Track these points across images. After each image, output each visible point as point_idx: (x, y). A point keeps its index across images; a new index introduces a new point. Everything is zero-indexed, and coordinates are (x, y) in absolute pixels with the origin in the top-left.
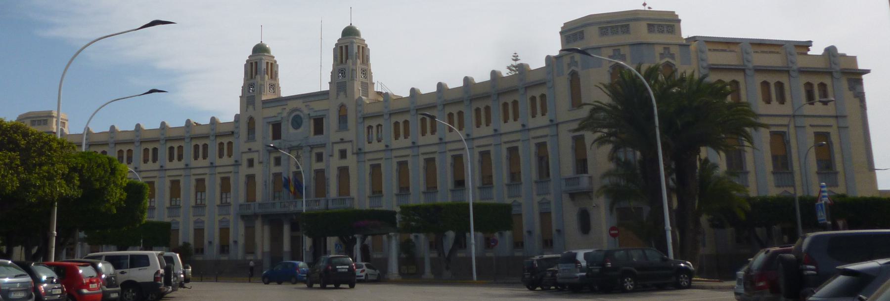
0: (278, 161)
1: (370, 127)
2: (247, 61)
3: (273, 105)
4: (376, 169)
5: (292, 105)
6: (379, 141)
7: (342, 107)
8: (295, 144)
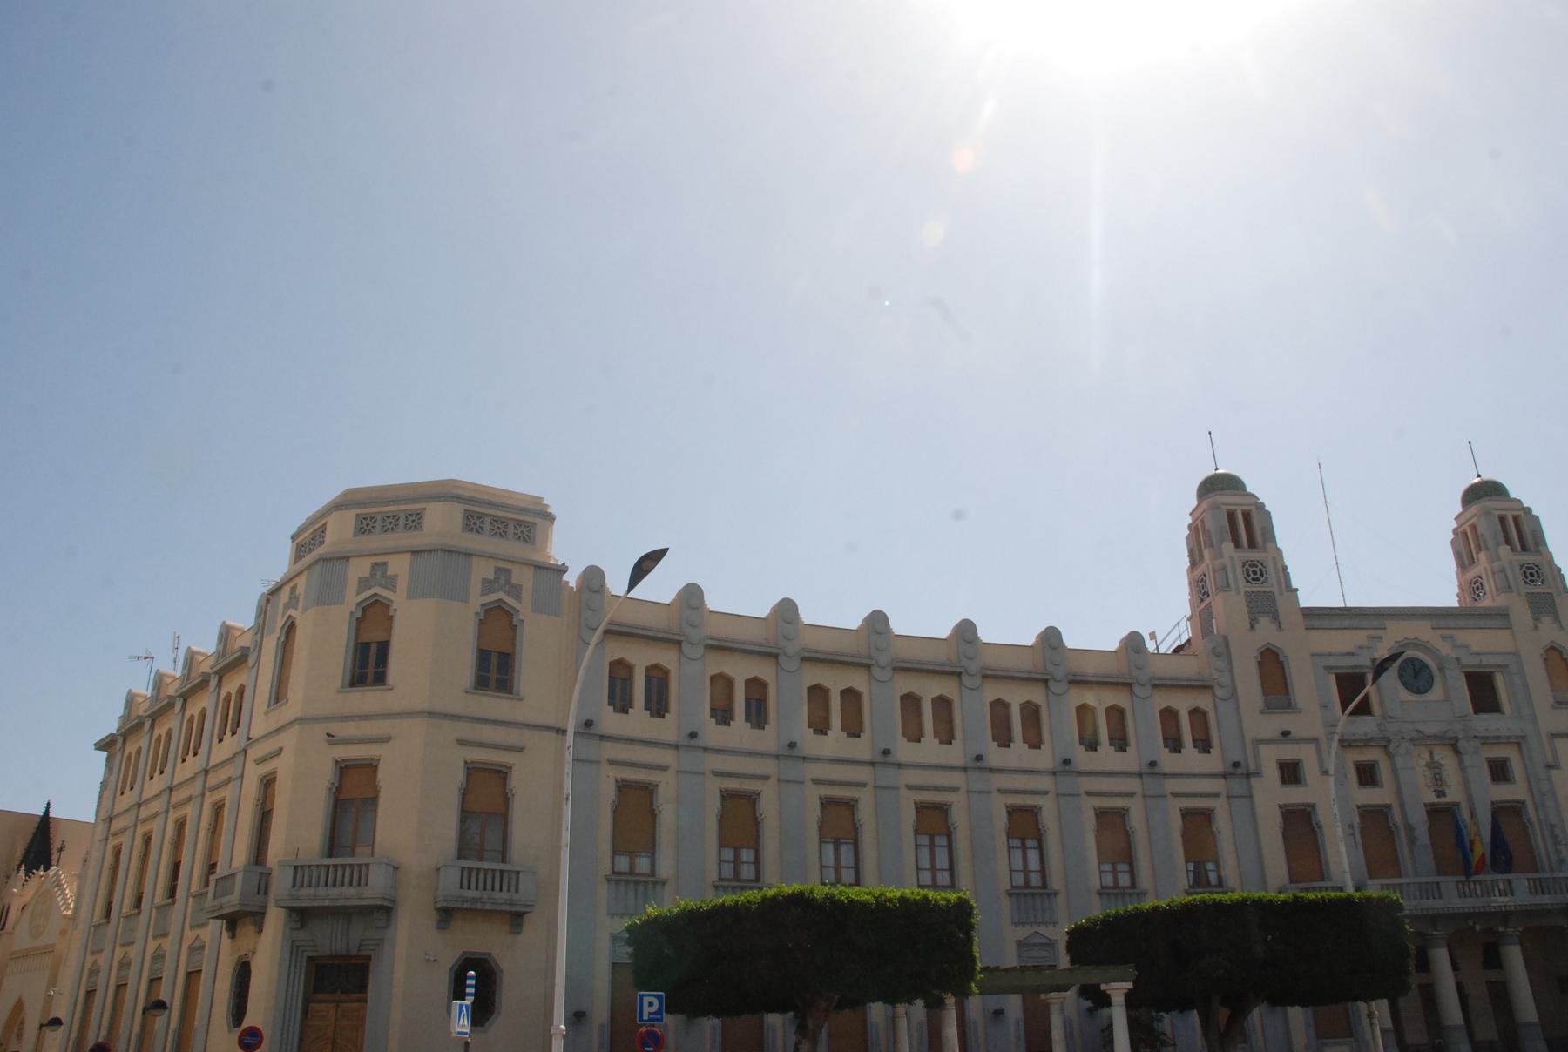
0: (1367, 775)
3: (1336, 623)
8: (1431, 729)
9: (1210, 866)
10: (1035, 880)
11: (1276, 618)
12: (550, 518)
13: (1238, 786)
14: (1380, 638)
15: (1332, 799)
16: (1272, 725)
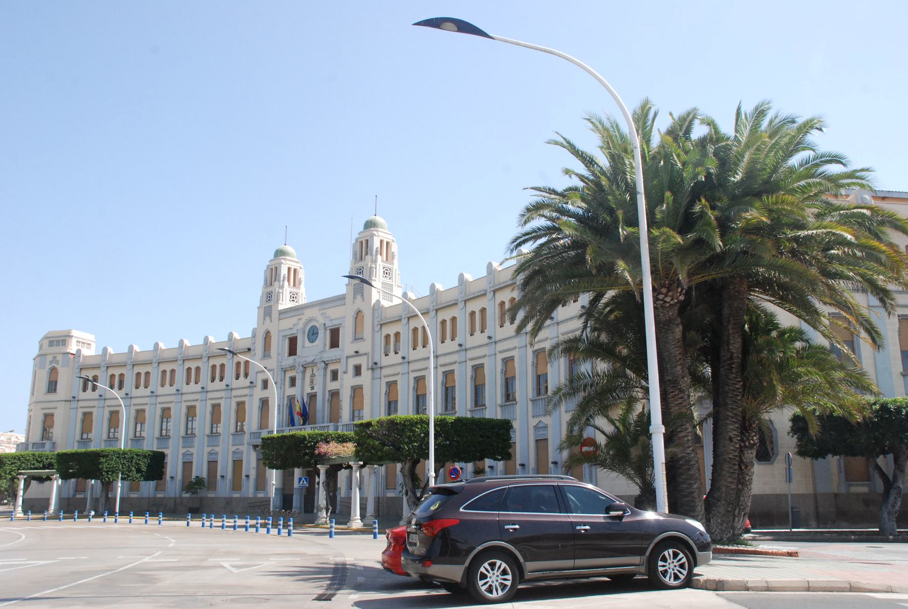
1: (387, 337)
2: (268, 267)
3: (290, 315)
4: (391, 386)
5: (308, 314)
6: (396, 353)
7: (359, 312)
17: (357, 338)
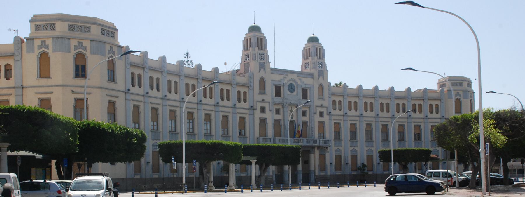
0: (277, 112)
5: (290, 76)
8: (293, 102)
9: (243, 131)
10: (209, 132)
11: (265, 70)
12: (117, 30)
13: (251, 112)
14: (286, 78)
15: (270, 117)
16: (259, 98)
17: (322, 98)
